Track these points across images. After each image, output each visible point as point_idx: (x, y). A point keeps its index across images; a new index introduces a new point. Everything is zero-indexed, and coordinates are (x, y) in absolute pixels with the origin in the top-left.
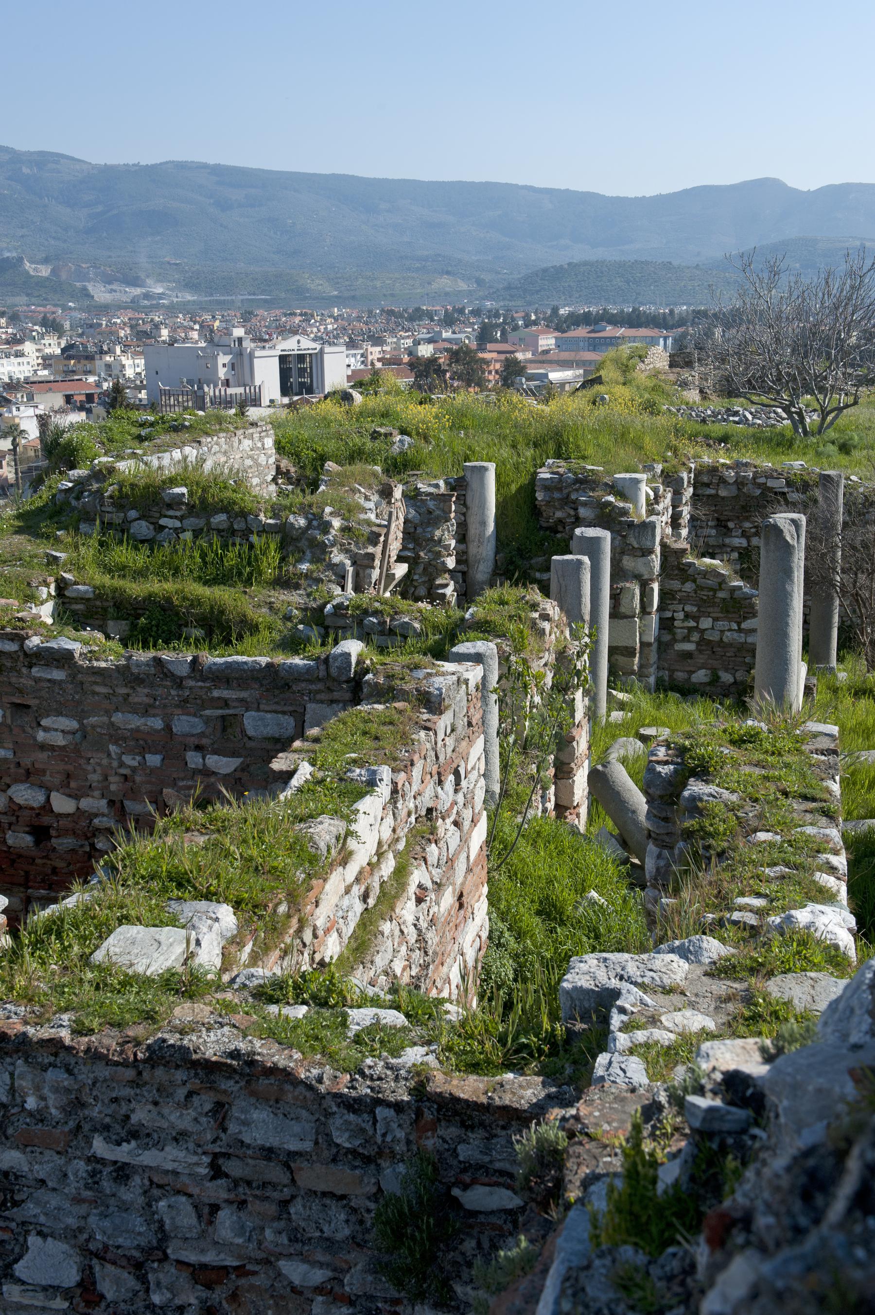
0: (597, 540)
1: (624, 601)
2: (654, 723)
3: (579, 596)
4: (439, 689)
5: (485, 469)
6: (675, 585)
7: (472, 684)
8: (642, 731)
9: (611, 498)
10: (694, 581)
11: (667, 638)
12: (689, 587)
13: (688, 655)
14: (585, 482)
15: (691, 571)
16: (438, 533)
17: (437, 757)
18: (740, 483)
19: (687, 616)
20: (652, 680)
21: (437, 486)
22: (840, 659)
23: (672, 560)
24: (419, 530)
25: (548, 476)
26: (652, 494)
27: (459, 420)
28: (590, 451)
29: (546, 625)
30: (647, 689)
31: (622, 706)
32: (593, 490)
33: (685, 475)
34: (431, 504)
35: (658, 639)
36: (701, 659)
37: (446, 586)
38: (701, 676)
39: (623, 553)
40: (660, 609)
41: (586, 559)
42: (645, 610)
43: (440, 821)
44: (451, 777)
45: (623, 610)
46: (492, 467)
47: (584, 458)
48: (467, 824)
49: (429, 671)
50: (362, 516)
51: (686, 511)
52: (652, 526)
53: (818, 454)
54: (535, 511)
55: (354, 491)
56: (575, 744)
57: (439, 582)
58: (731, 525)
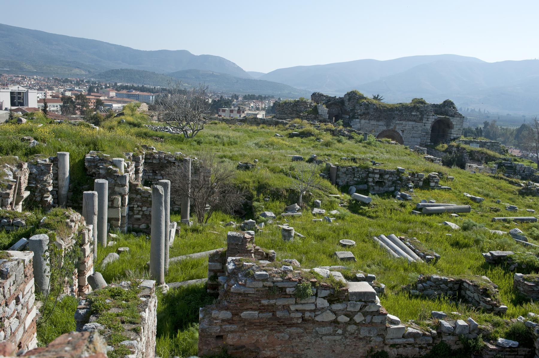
0: (102, 185)
1: (115, 202)
2: (124, 246)
3: (93, 206)
4: (7, 269)
5: (65, 155)
6: (134, 196)
7: (27, 262)
8: (119, 249)
9: (111, 167)
10: (141, 195)
11: (131, 213)
12: (139, 197)
13: (138, 219)
14: (103, 160)
15: (139, 191)
16: (45, 178)
17: (4, 297)
18: (160, 159)
19: (138, 206)
20: (126, 229)
21: (45, 161)
22: (191, 216)
23: (133, 187)
24: (38, 177)
25: (90, 157)
26: (126, 165)
27: (58, 134)
28: (106, 148)
29: (73, 224)
30: (122, 232)
31: (113, 239)
32: (105, 163)
33: (141, 157)
34: (43, 168)
35: (128, 214)
36: (143, 220)
37: (48, 197)
38: (143, 226)
39: (115, 186)
40: (128, 204)
41: (96, 193)
42: (123, 205)
43: (6, 320)
44: (14, 301)
45: (115, 205)
46: (68, 154)
47: (104, 151)
48: (23, 316)
49: (5, 260)
50: (6, 178)
51: (141, 168)
52: (125, 177)
53: (191, 145)
54: (85, 169)
55: (4, 167)
56: (86, 264)
57: (45, 196)
58: (157, 172)
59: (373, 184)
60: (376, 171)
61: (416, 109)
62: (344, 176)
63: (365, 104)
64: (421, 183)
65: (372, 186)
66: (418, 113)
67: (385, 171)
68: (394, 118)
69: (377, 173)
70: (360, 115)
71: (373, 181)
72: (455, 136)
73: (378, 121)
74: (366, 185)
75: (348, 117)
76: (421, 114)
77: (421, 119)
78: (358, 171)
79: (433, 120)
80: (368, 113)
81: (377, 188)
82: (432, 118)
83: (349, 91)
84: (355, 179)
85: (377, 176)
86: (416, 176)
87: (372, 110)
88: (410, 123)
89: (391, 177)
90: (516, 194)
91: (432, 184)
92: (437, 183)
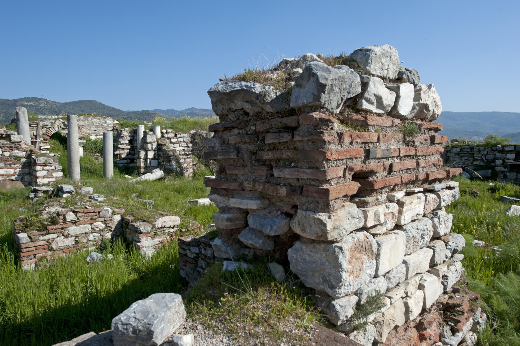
60: (506, 149)
65: (503, 172)
69: (510, 152)
71: (504, 165)
74: (490, 171)
78: (479, 151)
84: (475, 163)
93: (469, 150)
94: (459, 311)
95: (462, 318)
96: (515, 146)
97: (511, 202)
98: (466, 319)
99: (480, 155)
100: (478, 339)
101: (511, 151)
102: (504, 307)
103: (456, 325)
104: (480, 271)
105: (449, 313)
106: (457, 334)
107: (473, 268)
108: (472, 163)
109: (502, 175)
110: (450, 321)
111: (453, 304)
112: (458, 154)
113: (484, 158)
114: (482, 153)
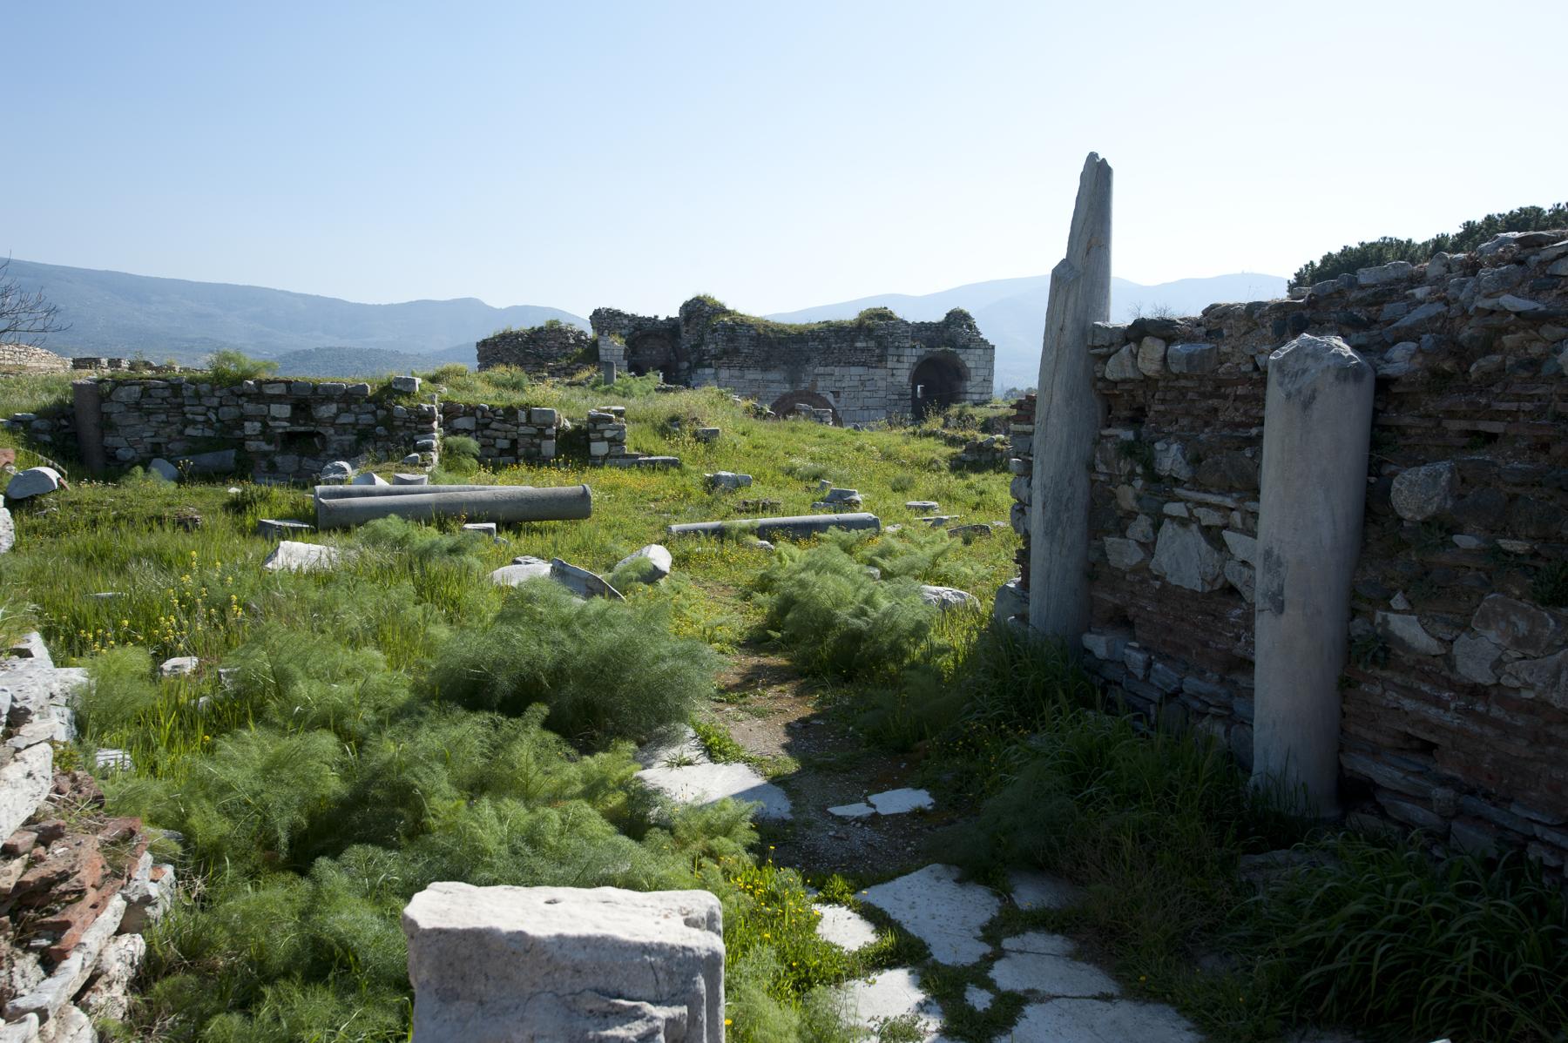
59: (265, 447)
60: (269, 390)
61: (871, 335)
62: (133, 418)
63: (725, 325)
64: (549, 447)
65: (265, 455)
66: (872, 344)
67: (315, 388)
68: (808, 360)
69: (277, 399)
70: (716, 357)
71: (266, 434)
72: (976, 397)
73: (765, 369)
74: (233, 453)
75: (686, 365)
76: (879, 345)
77: (882, 359)
78: (198, 395)
79: (914, 360)
80: (737, 351)
81: (287, 461)
82: (912, 355)
83: (689, 297)
84: (189, 431)
85: (283, 410)
86: (522, 416)
87: (745, 341)
88: (854, 370)
89: (348, 411)
90: (940, 469)
91: (599, 448)
92: (616, 442)
93: (166, 394)
94: (66, 893)
95: (72, 914)
96: (288, 383)
97: (284, 534)
98: (94, 906)
99: (200, 409)
100: (149, 946)
101: (280, 396)
102: (222, 827)
103: (56, 941)
104: (168, 750)
105: (32, 913)
106: (65, 964)
107: (147, 742)
108: (181, 433)
109: (264, 464)
110: (37, 936)
111: (42, 878)
112: (137, 406)
113: (214, 418)
114: (205, 401)
